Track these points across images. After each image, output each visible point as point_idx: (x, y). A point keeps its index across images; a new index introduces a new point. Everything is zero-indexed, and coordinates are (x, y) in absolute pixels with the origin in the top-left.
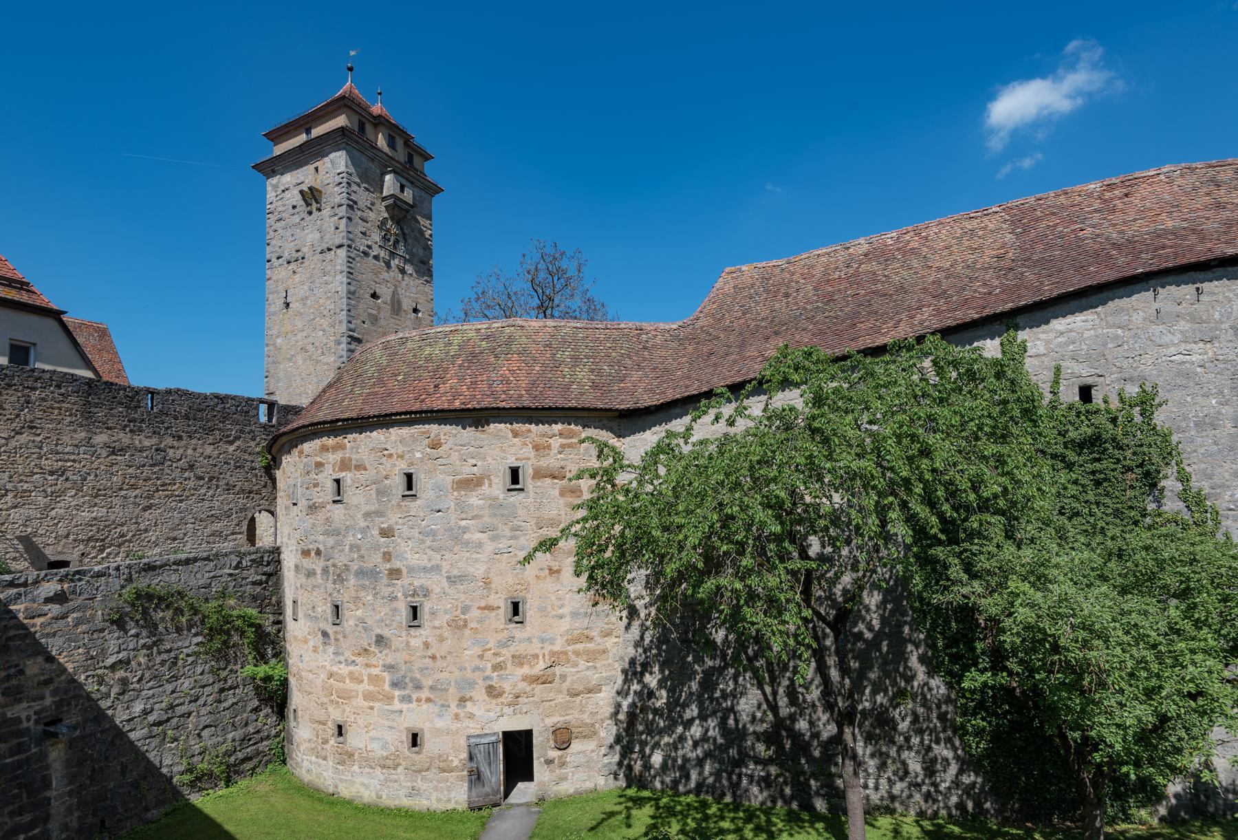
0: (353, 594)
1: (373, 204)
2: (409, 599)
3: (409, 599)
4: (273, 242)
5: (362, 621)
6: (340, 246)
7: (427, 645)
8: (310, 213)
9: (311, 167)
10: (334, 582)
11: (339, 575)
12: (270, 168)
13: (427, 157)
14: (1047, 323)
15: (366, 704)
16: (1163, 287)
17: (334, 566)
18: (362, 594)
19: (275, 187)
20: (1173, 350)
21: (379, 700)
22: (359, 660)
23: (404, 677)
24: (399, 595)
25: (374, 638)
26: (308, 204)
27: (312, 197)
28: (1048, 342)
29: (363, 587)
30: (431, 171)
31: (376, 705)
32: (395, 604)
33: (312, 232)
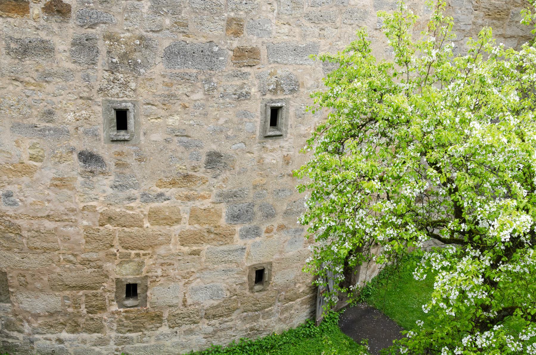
0: (161, 90)
2: (268, 96)
3: (268, 96)
5: (181, 134)
7: (287, 160)
10: (113, 68)
11: (124, 56)
15: (186, 249)
17: (109, 37)
18: (181, 90)
21: (208, 241)
22: (170, 191)
23: (251, 205)
24: (253, 90)
25: (204, 158)
29: (185, 78)
31: (205, 247)
32: (245, 105)
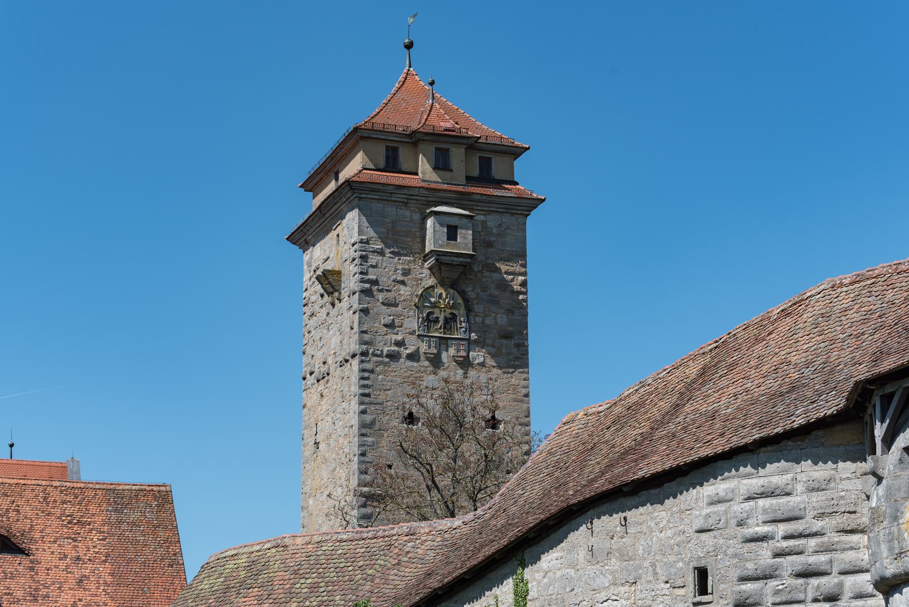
1: (406, 273)
4: (309, 350)
6: (354, 356)
8: (333, 305)
9: (333, 234)
12: (304, 236)
13: (516, 152)
14: (539, 559)
16: (599, 518)
19: (310, 266)
20: (602, 596)
26: (330, 294)
27: (330, 281)
28: (539, 582)
30: (527, 177)
33: (334, 335)
